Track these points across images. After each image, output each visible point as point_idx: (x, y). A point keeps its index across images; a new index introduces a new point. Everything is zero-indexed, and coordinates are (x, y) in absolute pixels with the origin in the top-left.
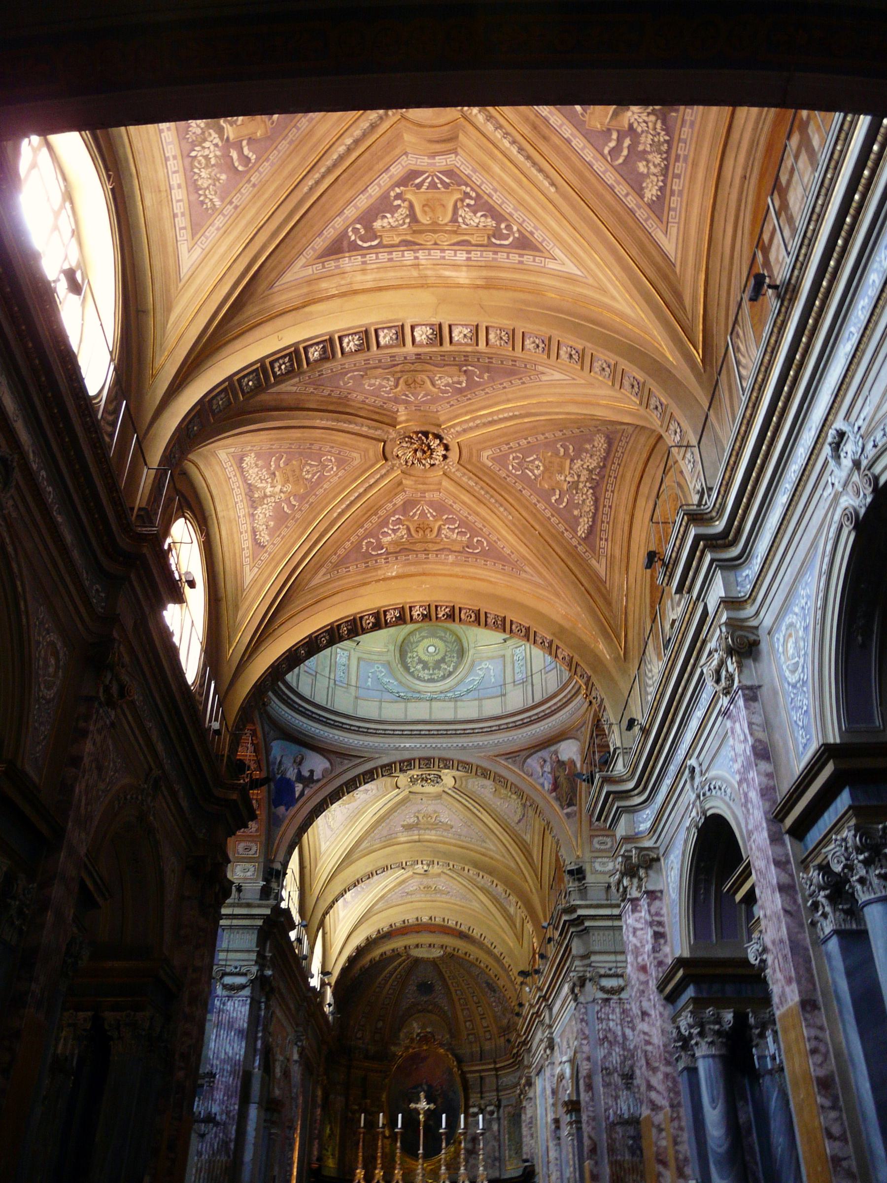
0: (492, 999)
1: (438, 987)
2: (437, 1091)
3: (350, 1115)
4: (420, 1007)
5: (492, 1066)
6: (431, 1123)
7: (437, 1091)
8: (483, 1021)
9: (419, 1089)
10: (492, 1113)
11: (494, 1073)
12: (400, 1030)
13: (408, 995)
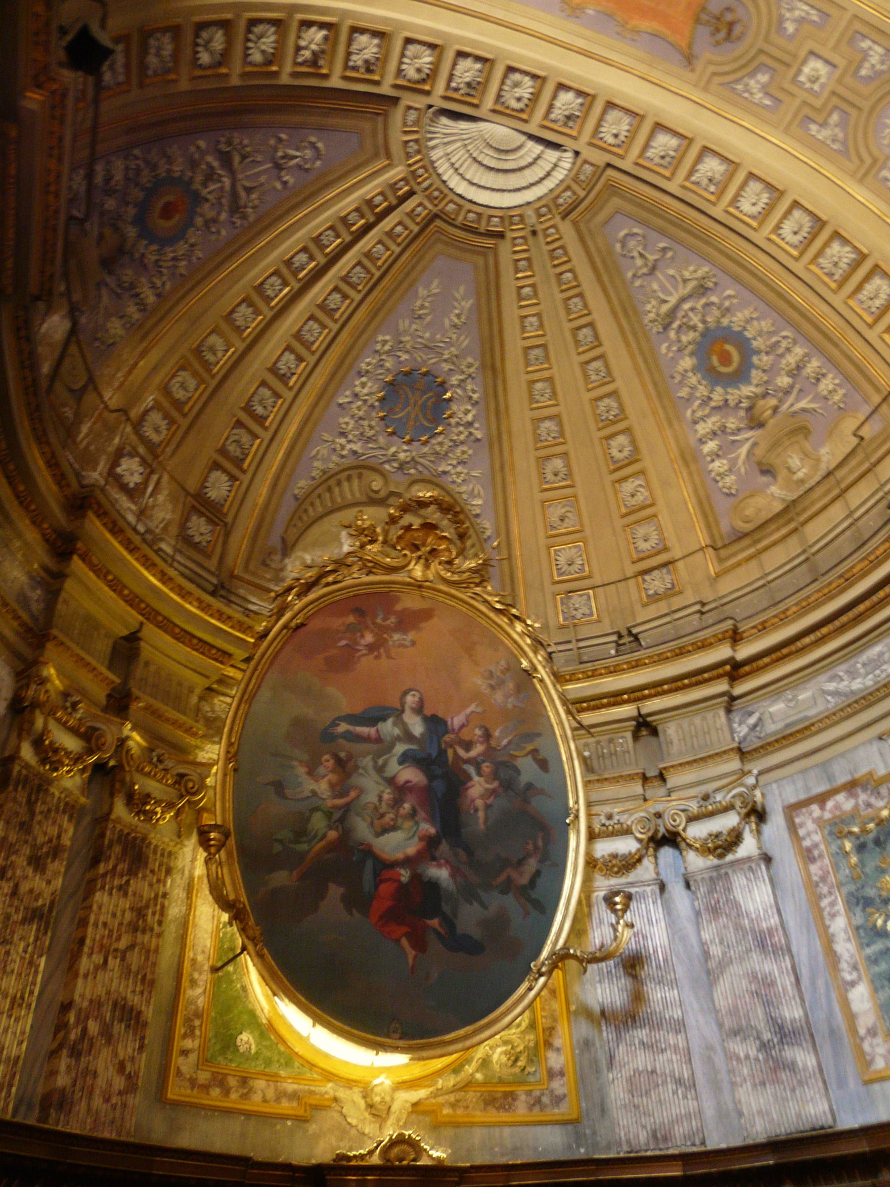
0: (703, 428)
1: (463, 412)
2: (468, 746)
3: (27, 752)
4: (376, 486)
5: (723, 652)
6: (441, 874)
7: (468, 746)
8: (641, 531)
9: (388, 728)
10: (735, 839)
11: (722, 686)
12: (287, 549)
13: (347, 422)
